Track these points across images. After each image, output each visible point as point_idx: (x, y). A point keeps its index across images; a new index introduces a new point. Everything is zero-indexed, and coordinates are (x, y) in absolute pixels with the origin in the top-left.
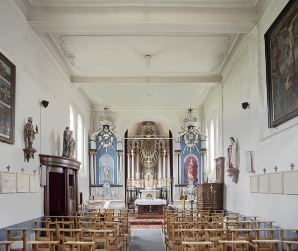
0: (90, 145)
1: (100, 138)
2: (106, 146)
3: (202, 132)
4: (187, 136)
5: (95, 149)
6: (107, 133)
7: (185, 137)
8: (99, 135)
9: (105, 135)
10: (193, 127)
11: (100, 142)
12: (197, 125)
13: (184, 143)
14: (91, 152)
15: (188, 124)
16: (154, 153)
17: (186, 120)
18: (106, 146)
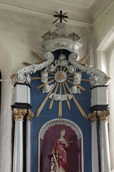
4: (51, 75)
7: (45, 75)
10: (67, 53)
12: (76, 47)
15: (53, 45)
17: (49, 35)
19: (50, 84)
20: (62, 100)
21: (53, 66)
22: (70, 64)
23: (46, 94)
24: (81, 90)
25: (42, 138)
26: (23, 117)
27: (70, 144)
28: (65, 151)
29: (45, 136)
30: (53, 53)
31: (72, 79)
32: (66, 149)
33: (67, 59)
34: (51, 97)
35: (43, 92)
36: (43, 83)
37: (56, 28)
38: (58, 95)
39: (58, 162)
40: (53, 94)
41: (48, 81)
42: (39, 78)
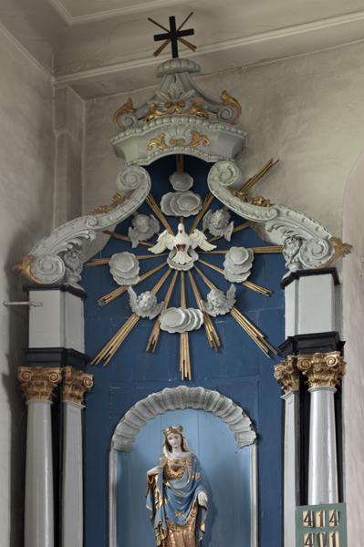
0: (20, 321)
1: (125, 268)
2: (173, 320)
6: (191, 223)
8: (118, 238)
9: (167, 240)
11: (125, 295)
18: (173, 320)
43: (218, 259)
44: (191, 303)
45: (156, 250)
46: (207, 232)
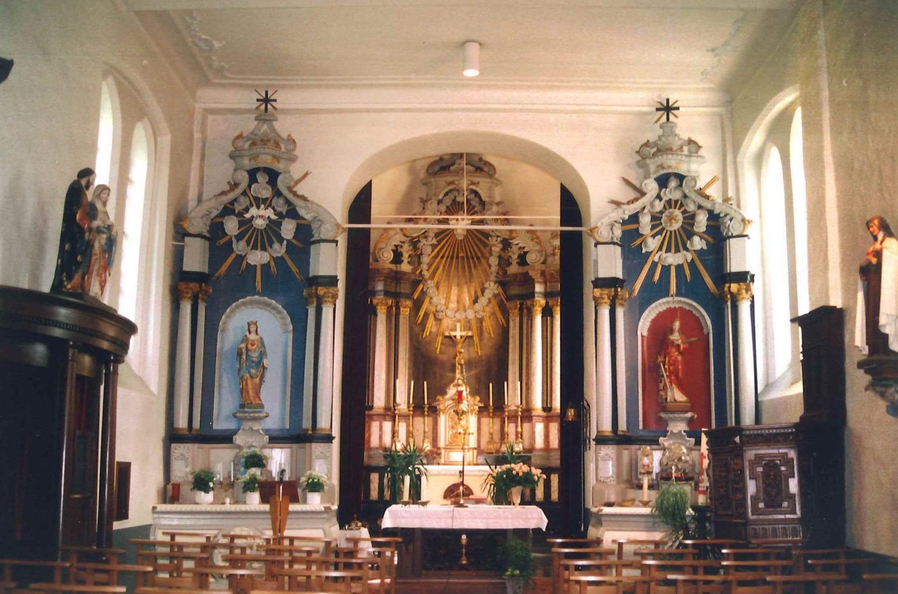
0: (177, 256)
1: (231, 226)
2: (257, 258)
3: (726, 200)
5: (206, 270)
7: (645, 220)
8: (228, 210)
9: (253, 211)
10: (681, 178)
11: (231, 241)
13: (640, 247)
14: (182, 286)
16: (488, 294)
18: (257, 258)
19: (654, 236)
20: (676, 263)
21: (657, 201)
22: (685, 196)
23: (649, 254)
24: (708, 243)
25: (645, 334)
26: (609, 301)
27: (690, 343)
28: (680, 358)
29: (650, 330)
30: (655, 179)
31: (691, 222)
32: (680, 353)
33: (681, 185)
34: (656, 259)
35: (644, 251)
36: (642, 235)
37: (660, 132)
38: (669, 254)
39: (669, 377)
40: (659, 253)
41: (651, 229)
42: (635, 226)
43: (278, 224)
44: (264, 249)
45: (248, 216)
46: (274, 209)
